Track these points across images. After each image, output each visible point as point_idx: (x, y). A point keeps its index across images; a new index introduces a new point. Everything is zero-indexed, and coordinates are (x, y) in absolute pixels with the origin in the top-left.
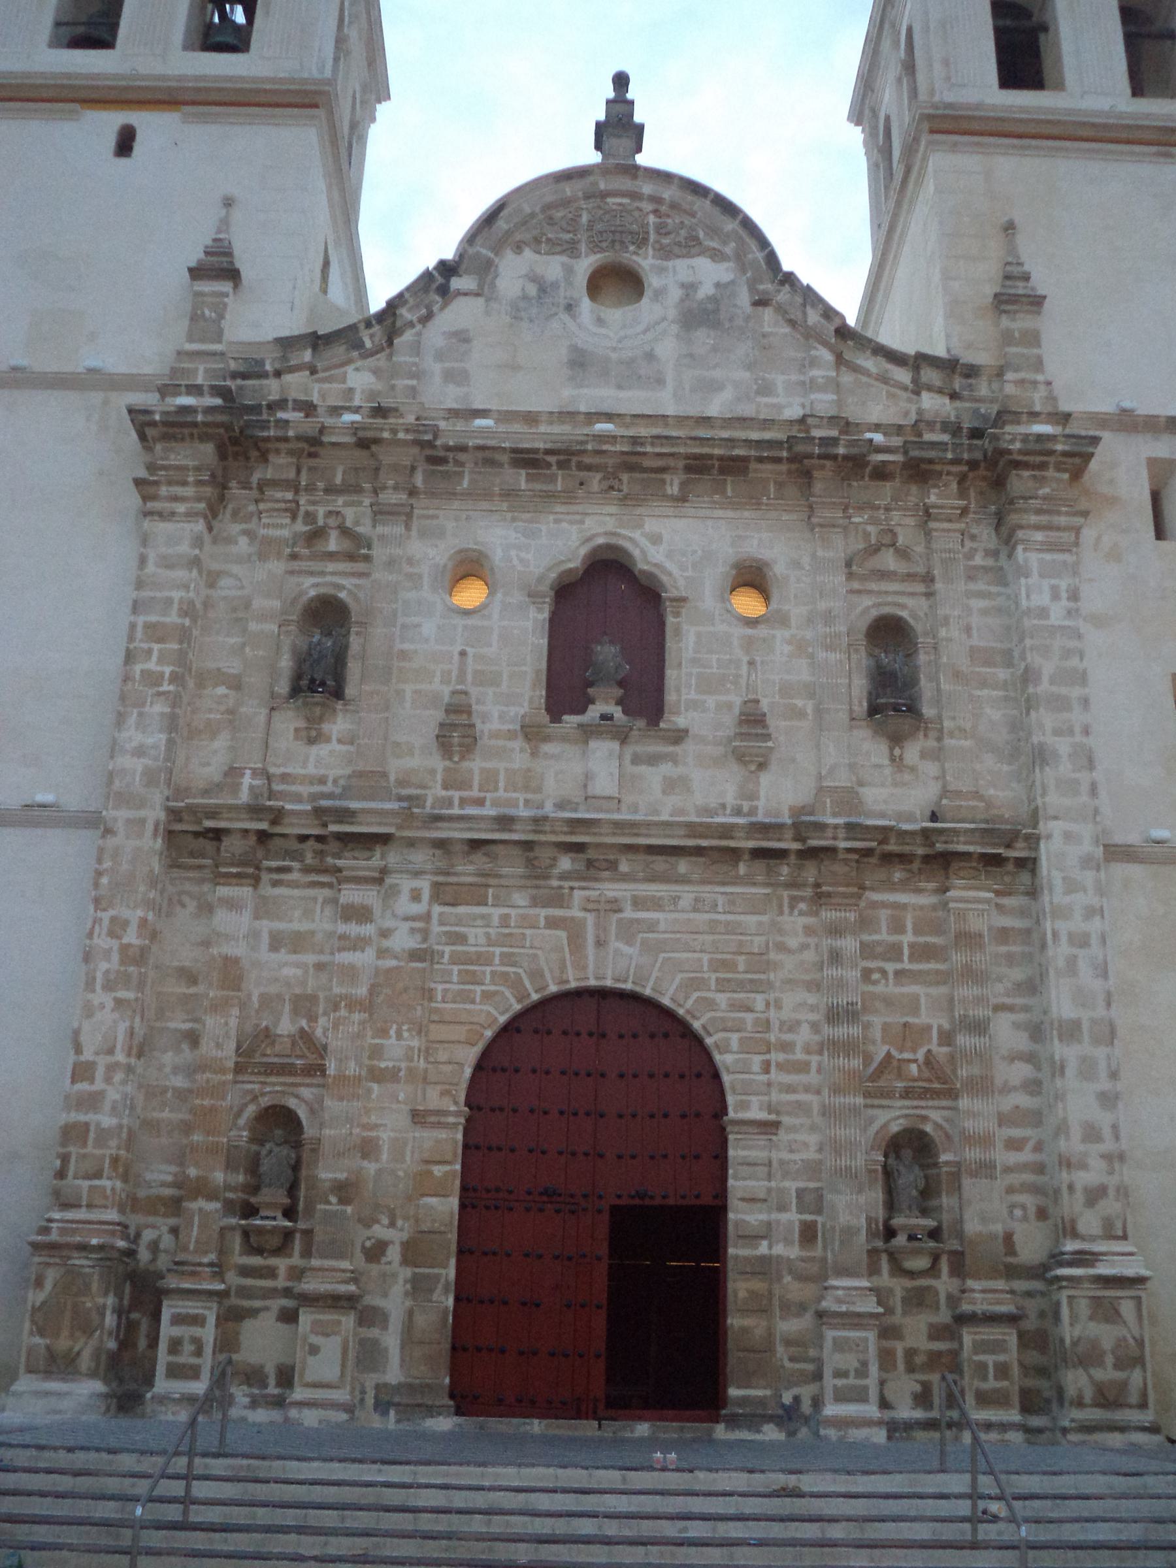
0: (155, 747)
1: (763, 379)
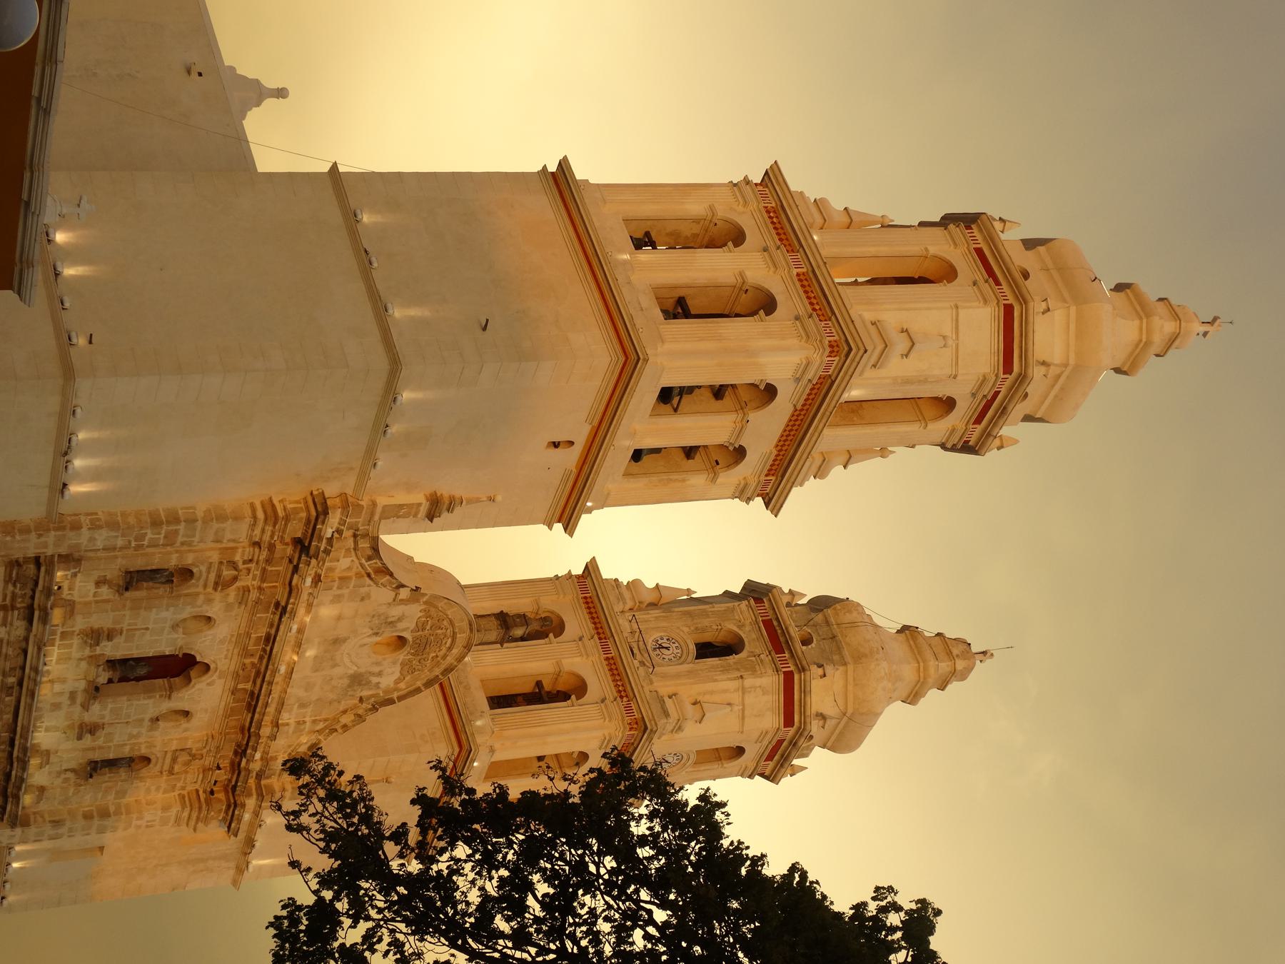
1: (310, 705)
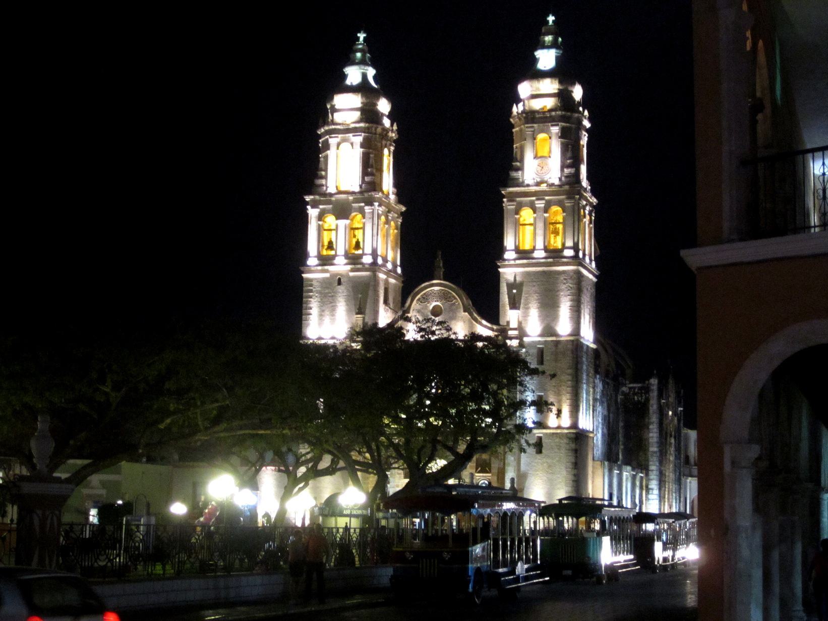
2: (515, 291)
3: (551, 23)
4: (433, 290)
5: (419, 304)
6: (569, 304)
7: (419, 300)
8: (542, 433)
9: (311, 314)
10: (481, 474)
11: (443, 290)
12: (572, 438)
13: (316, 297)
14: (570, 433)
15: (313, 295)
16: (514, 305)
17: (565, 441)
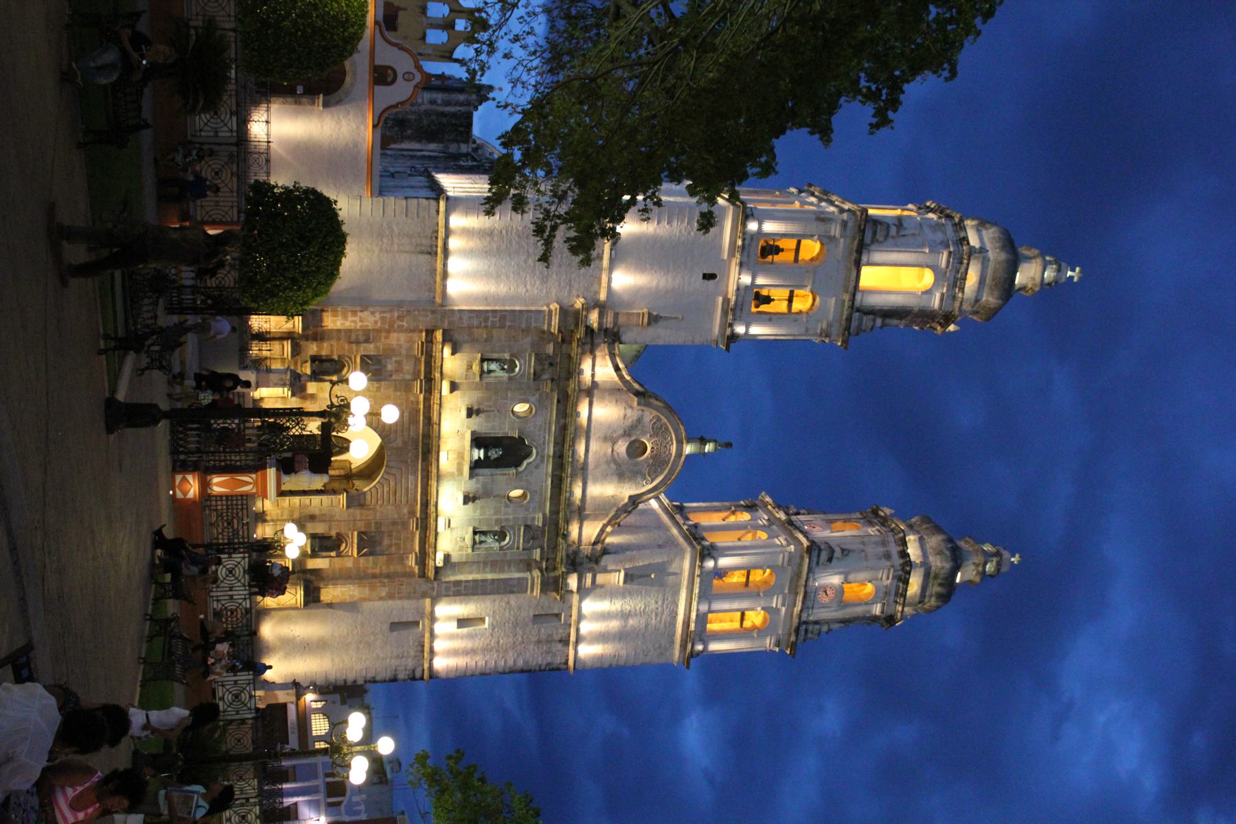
0: (462, 323)
2: (653, 576)
3: (1012, 559)
4: (672, 444)
5: (651, 420)
6: (623, 653)
7: (659, 419)
8: (423, 629)
9: (658, 223)
10: (356, 541)
11: (669, 460)
12: (414, 675)
13: (689, 233)
14: (423, 670)
15: (692, 227)
16: (629, 578)
17: (410, 663)
